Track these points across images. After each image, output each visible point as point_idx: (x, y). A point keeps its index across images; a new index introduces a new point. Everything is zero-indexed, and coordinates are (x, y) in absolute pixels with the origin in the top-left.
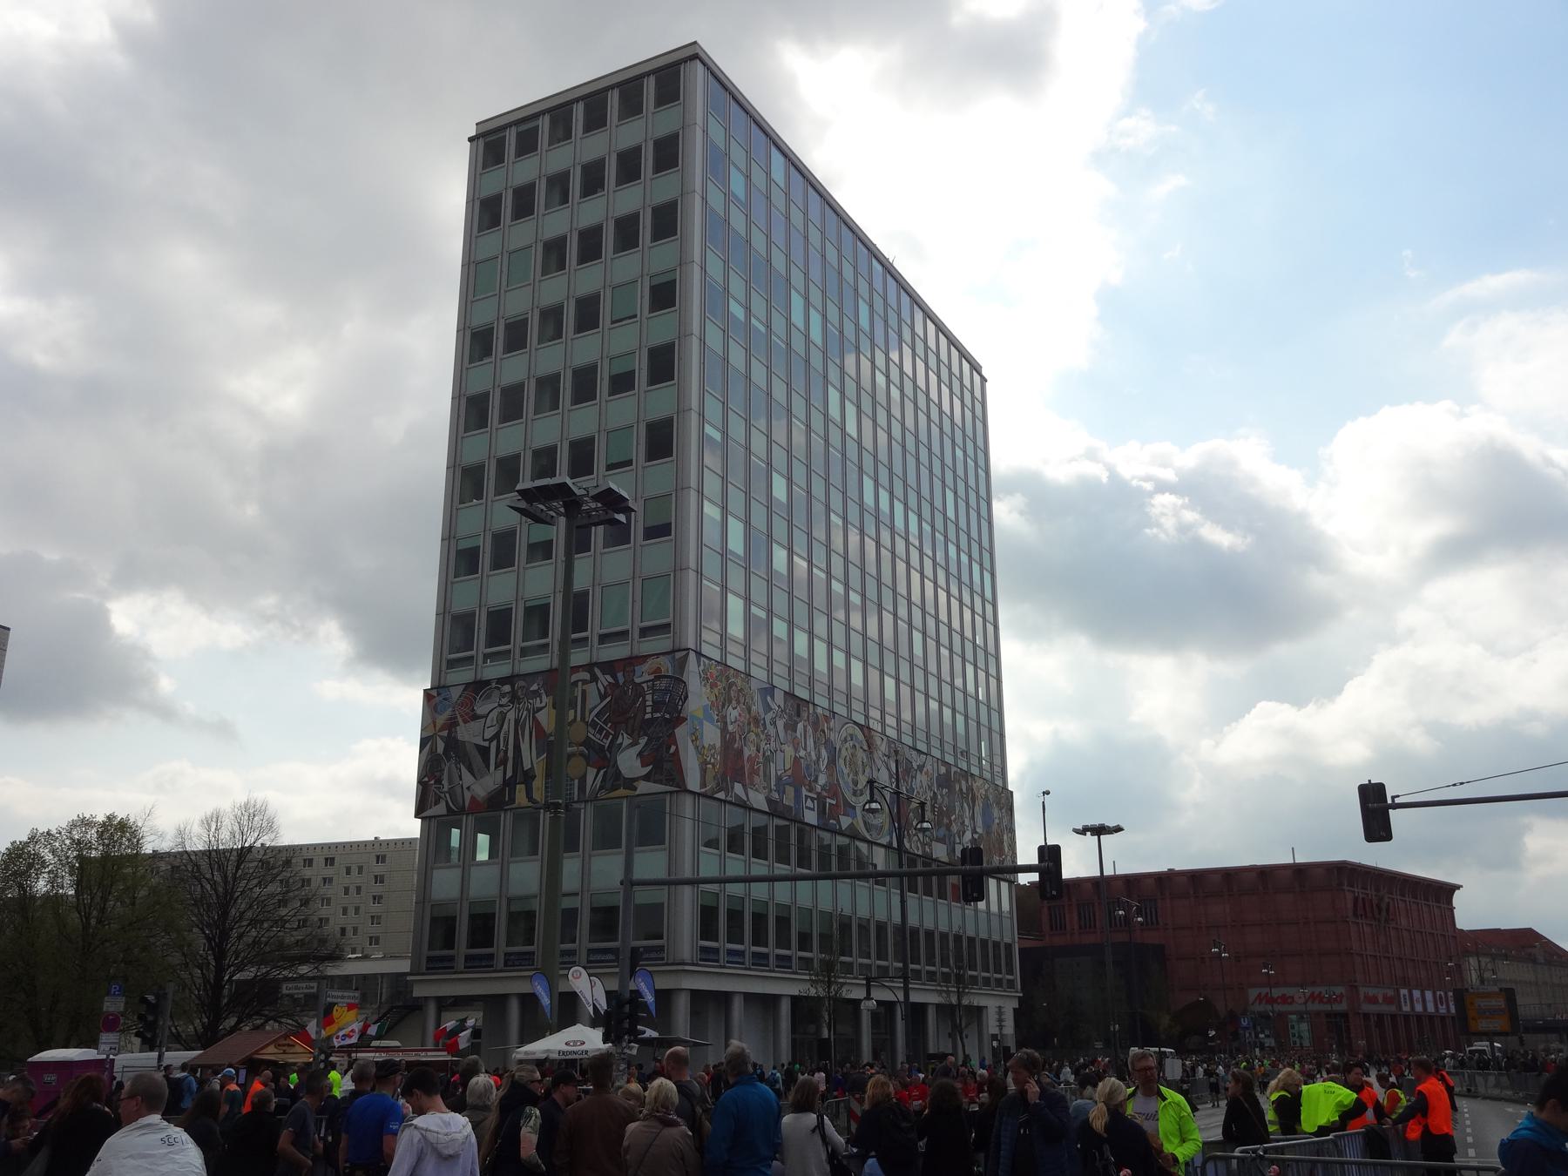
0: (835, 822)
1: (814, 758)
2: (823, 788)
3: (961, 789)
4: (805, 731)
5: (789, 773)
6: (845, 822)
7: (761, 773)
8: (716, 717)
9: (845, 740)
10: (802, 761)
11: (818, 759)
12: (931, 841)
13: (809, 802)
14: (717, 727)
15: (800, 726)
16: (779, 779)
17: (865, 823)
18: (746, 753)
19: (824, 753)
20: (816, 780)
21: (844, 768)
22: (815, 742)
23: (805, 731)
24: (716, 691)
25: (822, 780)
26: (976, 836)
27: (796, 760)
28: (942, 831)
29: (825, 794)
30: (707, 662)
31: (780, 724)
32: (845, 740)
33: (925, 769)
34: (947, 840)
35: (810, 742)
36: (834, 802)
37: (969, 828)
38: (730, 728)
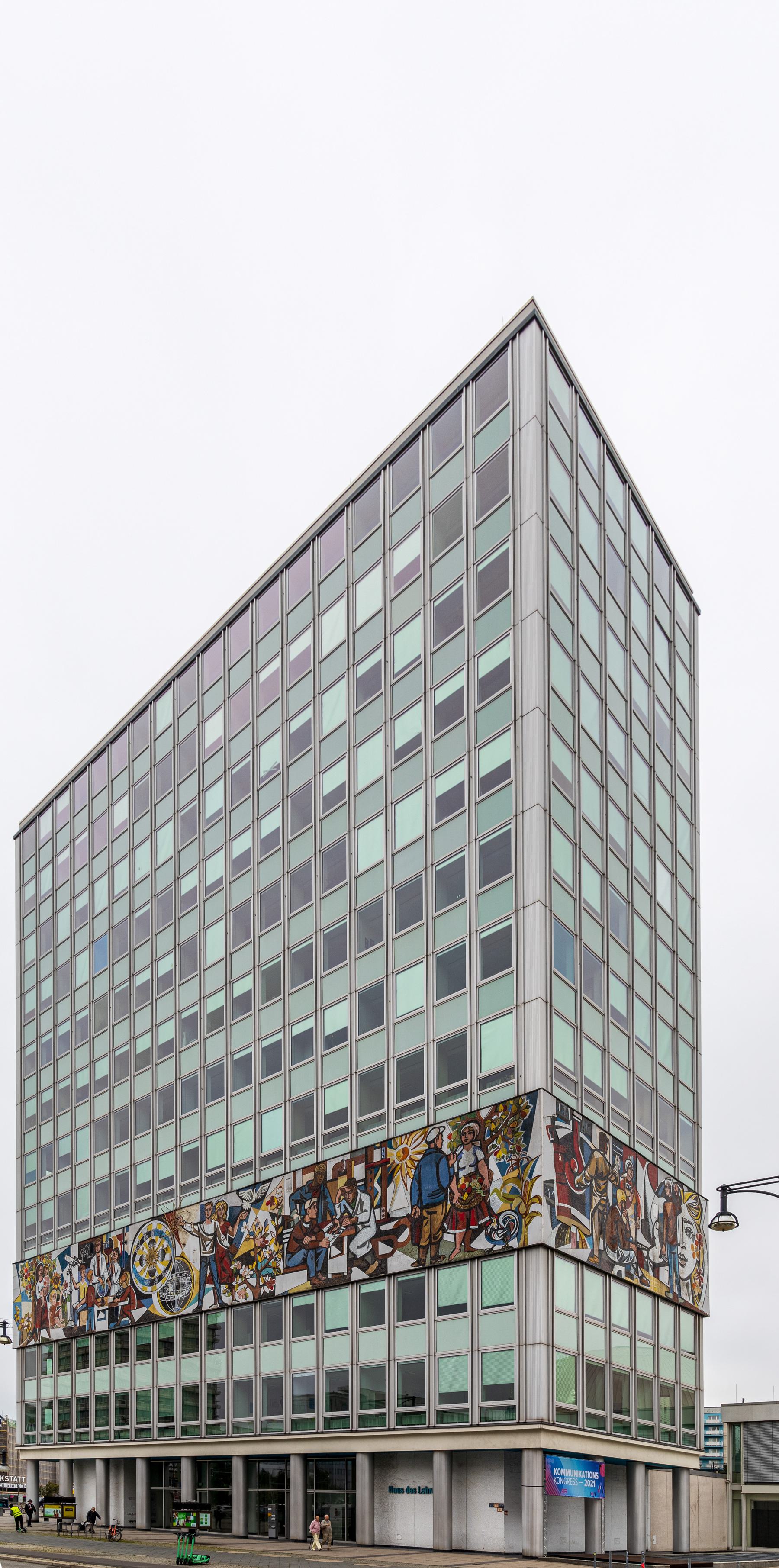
0: (127, 1319)
1: (106, 1276)
3: (352, 1182)
4: (98, 1261)
5: (84, 1301)
7: (60, 1314)
8: (29, 1295)
9: (142, 1242)
10: (95, 1286)
11: (111, 1276)
12: (273, 1277)
13: (101, 1315)
14: (30, 1301)
15: (94, 1260)
16: (74, 1310)
18: (49, 1305)
19: (117, 1267)
20: (108, 1294)
21: (139, 1269)
22: (107, 1264)
23: (98, 1261)
24: (29, 1279)
25: (115, 1290)
26: (390, 1226)
27: (90, 1288)
28: (299, 1256)
29: (117, 1300)
30: (22, 1264)
31: (75, 1270)
32: (142, 1242)
33: (268, 1199)
34: (311, 1263)
35: (104, 1267)
36: (126, 1303)
37: (372, 1223)
38: (38, 1296)
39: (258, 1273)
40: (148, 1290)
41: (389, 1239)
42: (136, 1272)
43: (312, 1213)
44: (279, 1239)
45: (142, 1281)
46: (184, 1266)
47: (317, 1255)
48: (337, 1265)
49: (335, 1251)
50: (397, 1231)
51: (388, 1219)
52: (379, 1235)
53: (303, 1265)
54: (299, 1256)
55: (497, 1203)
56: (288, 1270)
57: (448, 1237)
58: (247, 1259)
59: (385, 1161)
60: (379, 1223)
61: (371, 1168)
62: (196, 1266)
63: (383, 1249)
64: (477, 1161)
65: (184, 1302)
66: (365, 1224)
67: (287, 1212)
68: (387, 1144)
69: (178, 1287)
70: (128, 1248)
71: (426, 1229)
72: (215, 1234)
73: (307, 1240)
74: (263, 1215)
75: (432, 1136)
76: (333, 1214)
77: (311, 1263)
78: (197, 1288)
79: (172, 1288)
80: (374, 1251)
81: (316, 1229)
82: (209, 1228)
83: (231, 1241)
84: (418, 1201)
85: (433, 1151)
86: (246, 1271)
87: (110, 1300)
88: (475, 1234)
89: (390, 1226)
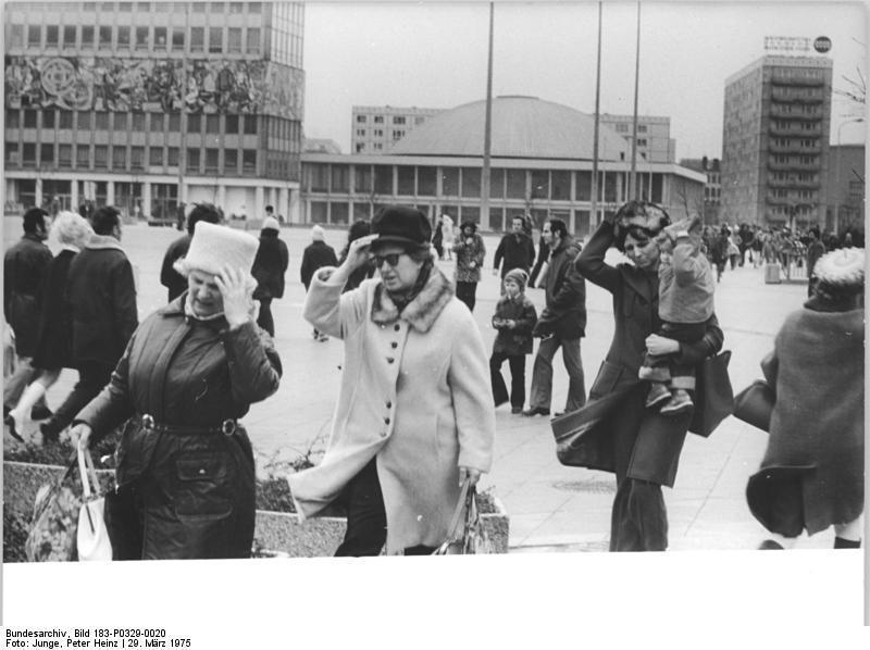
1: (20, 79)
2: (29, 91)
4: (13, 69)
6: (45, 104)
9: (51, 67)
17: (67, 102)
19: (30, 77)
20: (22, 89)
22: (22, 73)
25: (27, 87)
28: (157, 97)
33: (140, 66)
39: (132, 99)
40: (54, 93)
41: (206, 99)
42: (46, 83)
43: (165, 80)
44: (146, 86)
45: (50, 87)
46: (82, 85)
47: (167, 98)
48: (177, 104)
49: (177, 98)
50: (209, 97)
51: (204, 91)
52: (200, 96)
53: (159, 100)
54: (157, 97)
55: (252, 97)
56: (150, 101)
57: (232, 104)
58: (126, 91)
59: (203, 68)
60: (200, 92)
61: (196, 68)
62: (91, 85)
63: (201, 102)
64: (244, 80)
65: (83, 104)
66: (193, 91)
67: (150, 74)
68: (206, 60)
69: (77, 96)
70: (39, 68)
71: (222, 100)
72: (104, 76)
73: (162, 90)
74: (137, 72)
75: (226, 63)
76: (176, 83)
77: (163, 99)
78: (90, 98)
79: (73, 96)
80: (197, 103)
81: (167, 86)
82: (101, 71)
83: (115, 81)
84: (219, 87)
85: (226, 70)
86: (124, 96)
87: (23, 92)
88: (242, 106)
89: (203, 94)
